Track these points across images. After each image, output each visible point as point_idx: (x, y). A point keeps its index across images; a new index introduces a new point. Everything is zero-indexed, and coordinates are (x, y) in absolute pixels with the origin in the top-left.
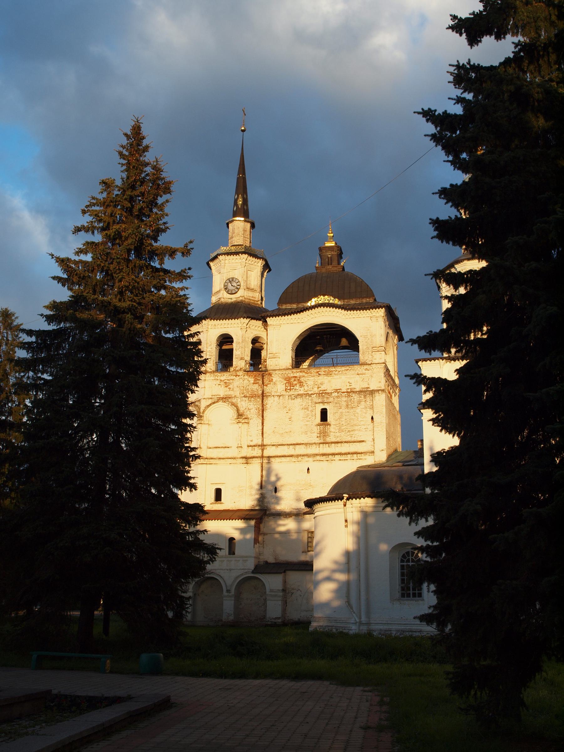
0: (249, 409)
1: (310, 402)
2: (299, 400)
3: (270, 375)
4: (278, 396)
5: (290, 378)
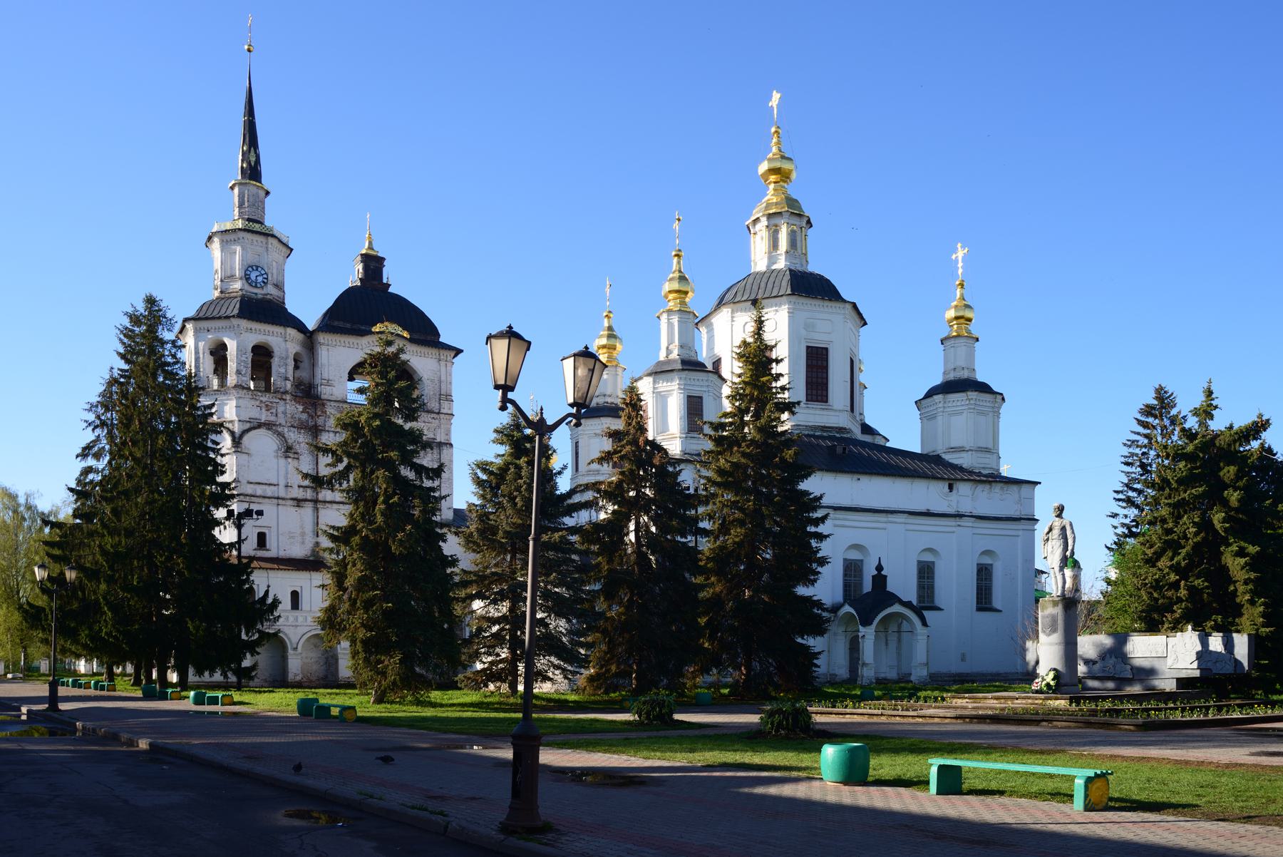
3: (323, 405)
4: (333, 432)
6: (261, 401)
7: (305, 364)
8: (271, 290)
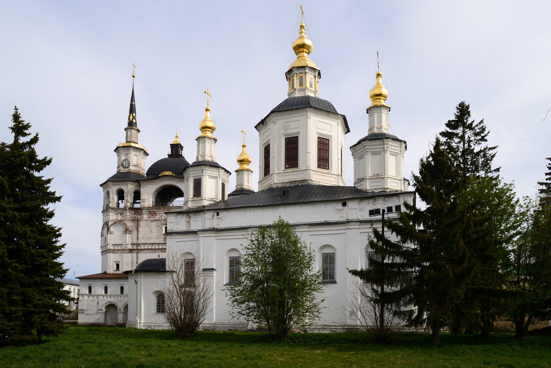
1: (160, 223)
2: (154, 223)
5: (151, 212)
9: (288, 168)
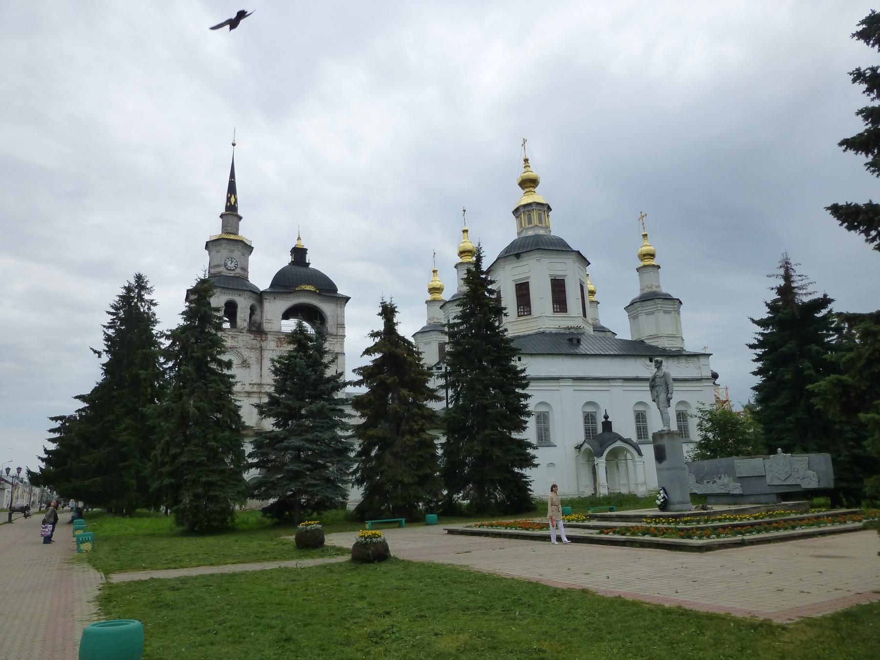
0: (250, 358)
4: (272, 350)
6: (229, 334)
7: (258, 312)
8: (238, 271)
9: (557, 312)
